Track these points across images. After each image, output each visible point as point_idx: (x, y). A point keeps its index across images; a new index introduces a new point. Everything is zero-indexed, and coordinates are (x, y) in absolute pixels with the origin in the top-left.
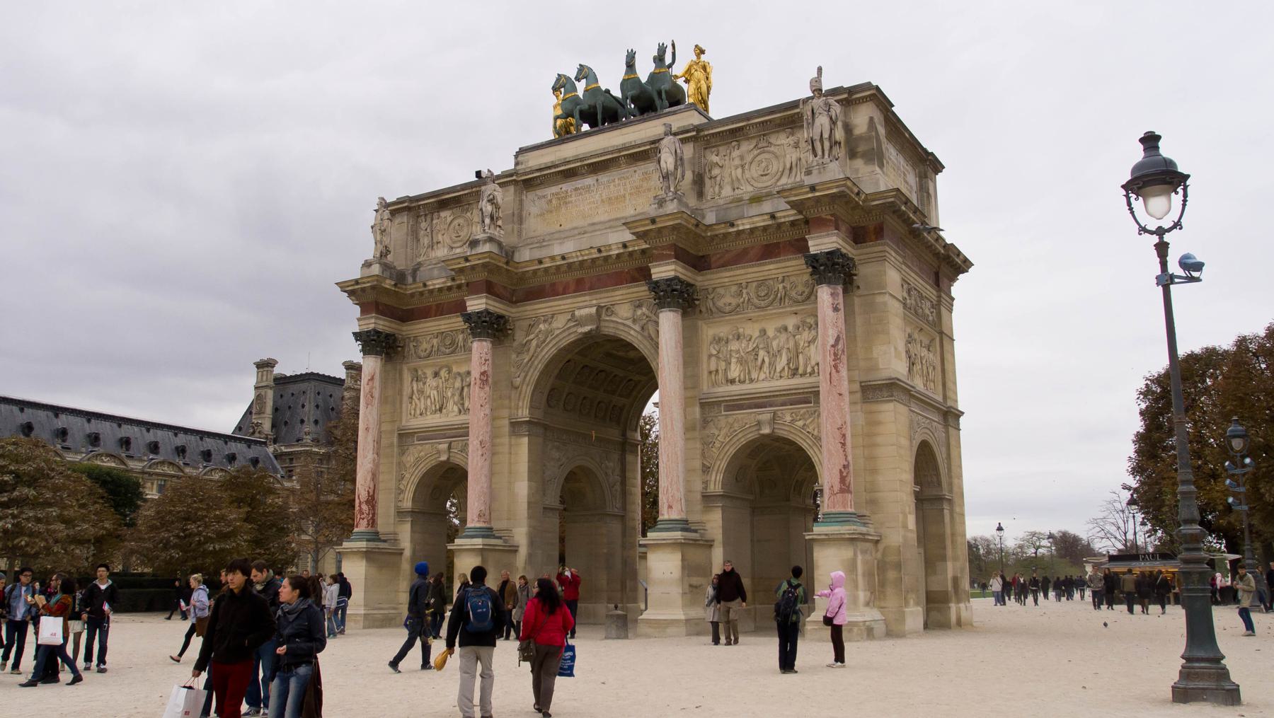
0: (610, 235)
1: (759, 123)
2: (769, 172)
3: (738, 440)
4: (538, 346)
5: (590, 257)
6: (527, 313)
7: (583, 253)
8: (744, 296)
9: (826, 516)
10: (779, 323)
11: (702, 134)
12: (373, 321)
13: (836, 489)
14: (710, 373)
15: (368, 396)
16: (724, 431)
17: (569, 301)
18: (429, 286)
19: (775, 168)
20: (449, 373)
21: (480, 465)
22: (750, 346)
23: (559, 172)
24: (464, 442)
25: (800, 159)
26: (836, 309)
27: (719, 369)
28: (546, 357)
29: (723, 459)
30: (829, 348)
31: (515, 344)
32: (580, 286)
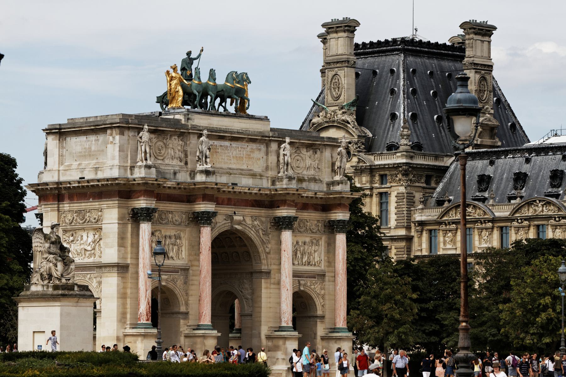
0: (243, 179)
5: (244, 191)
17: (226, 209)
19: (302, 165)
32: (229, 202)
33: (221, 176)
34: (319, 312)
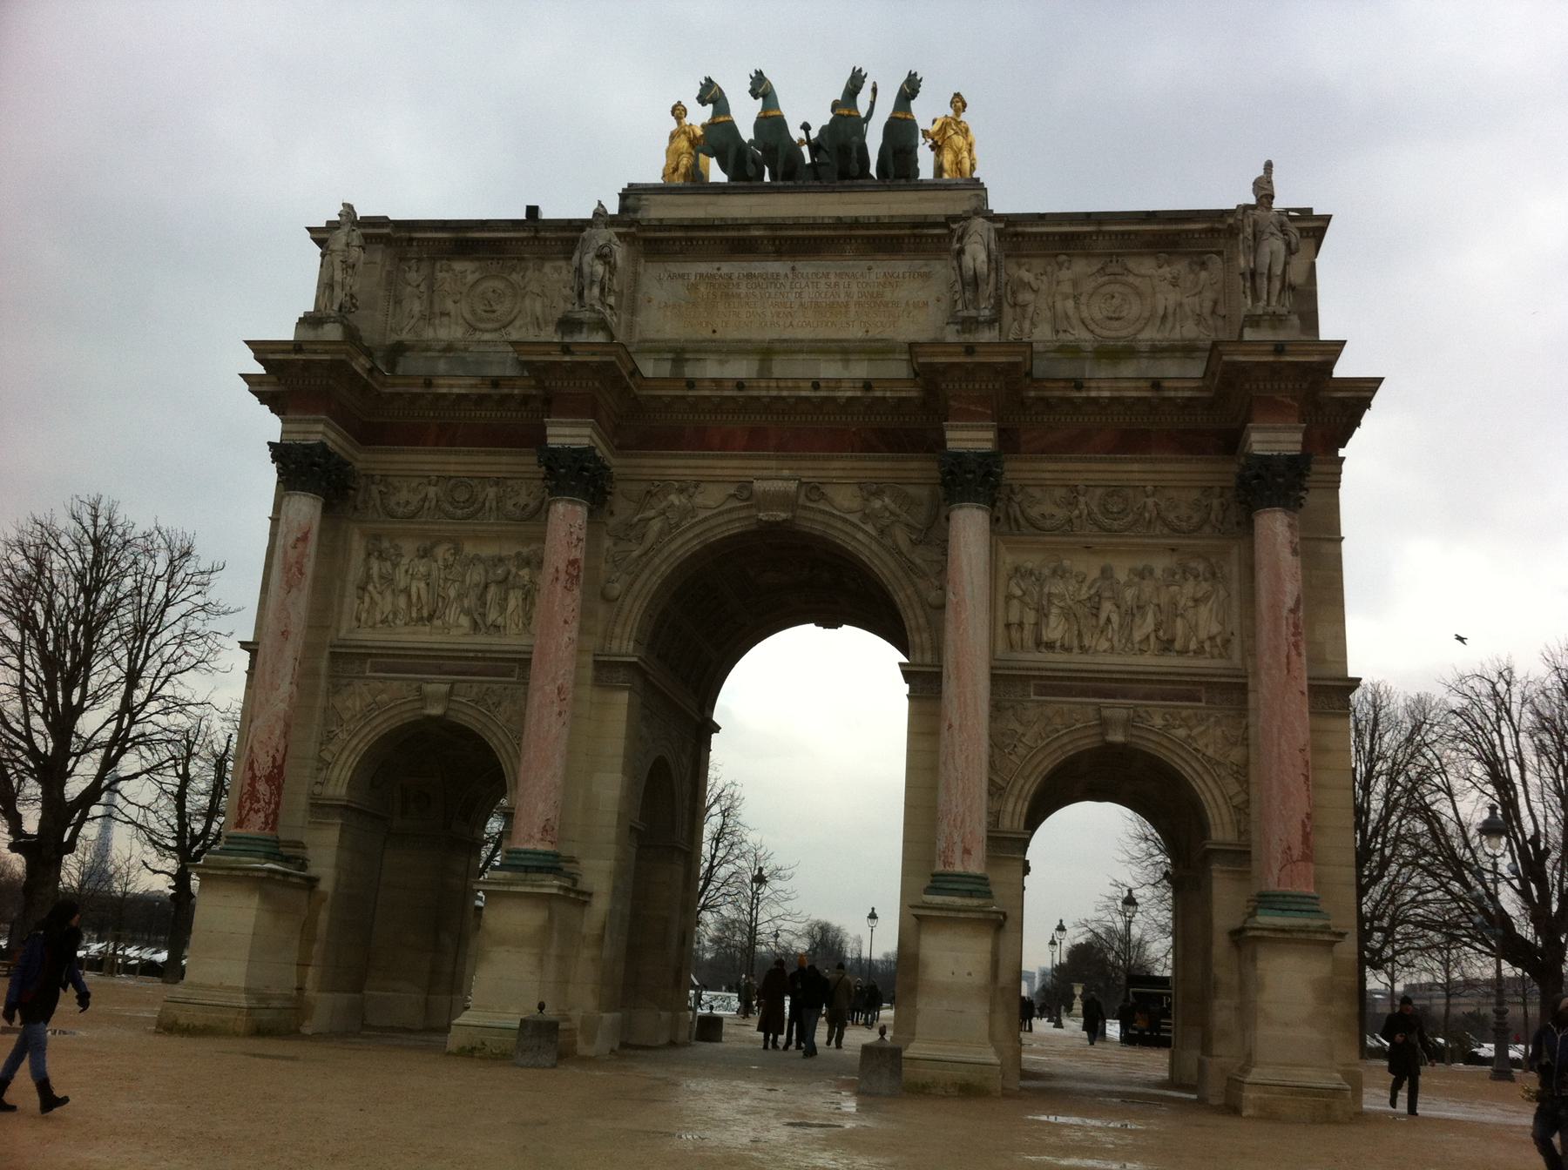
0: (823, 365)
1: (1116, 233)
2: (1124, 314)
3: (1060, 747)
4: (661, 533)
5: (794, 393)
6: (645, 471)
7: (782, 384)
8: (1082, 506)
9: (1262, 899)
10: (1139, 563)
11: (1011, 229)
12: (321, 427)
13: (1297, 853)
14: (1008, 626)
15: (294, 569)
16: (1035, 726)
17: (736, 463)
18: (442, 386)
20: (455, 554)
21: (554, 731)
22: (1083, 592)
23: (722, 239)
24: (487, 685)
25: (1181, 305)
26: (1295, 552)
27: (1025, 621)
28: (679, 554)
29: (1029, 777)
30: (1285, 612)
31: (612, 521)
32: (756, 441)
33: (721, 362)
34: (1221, 831)
